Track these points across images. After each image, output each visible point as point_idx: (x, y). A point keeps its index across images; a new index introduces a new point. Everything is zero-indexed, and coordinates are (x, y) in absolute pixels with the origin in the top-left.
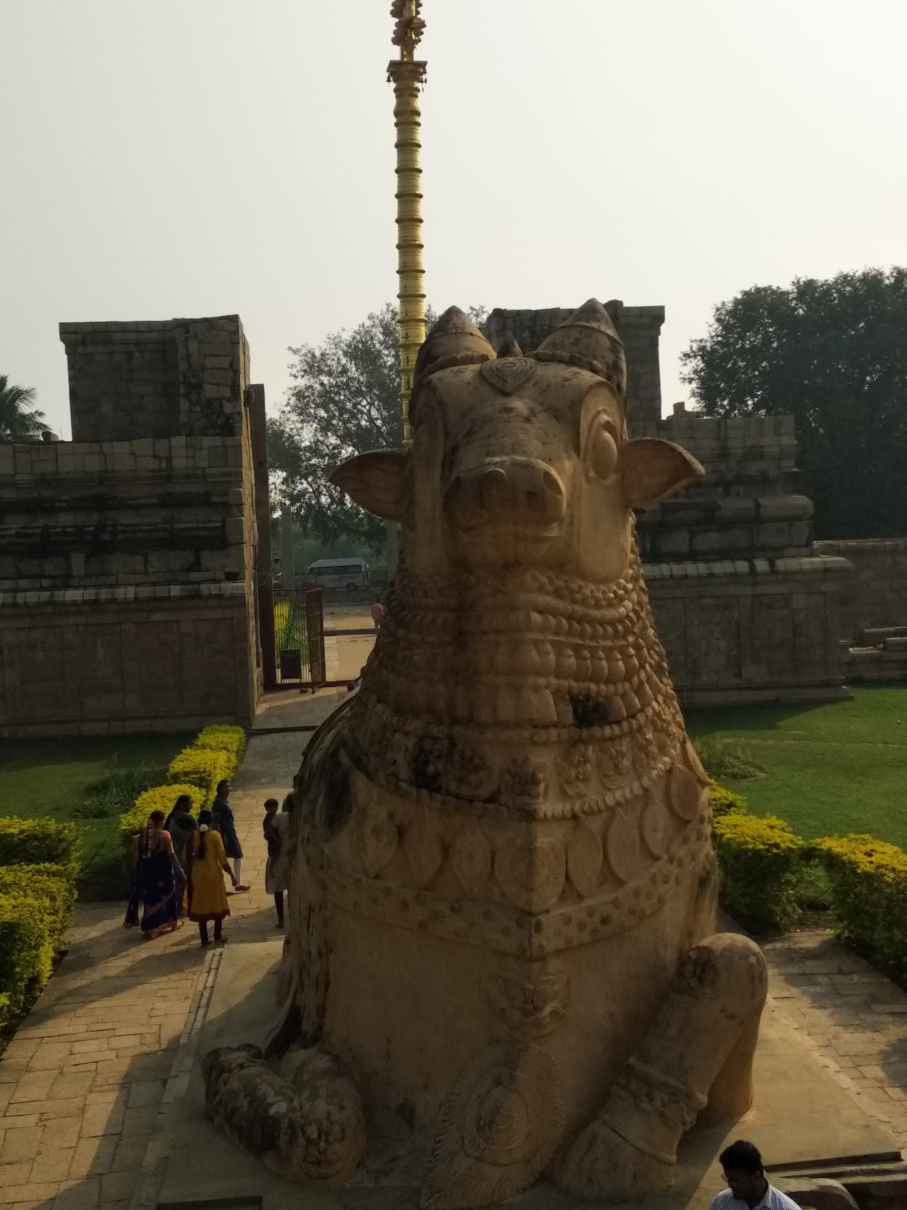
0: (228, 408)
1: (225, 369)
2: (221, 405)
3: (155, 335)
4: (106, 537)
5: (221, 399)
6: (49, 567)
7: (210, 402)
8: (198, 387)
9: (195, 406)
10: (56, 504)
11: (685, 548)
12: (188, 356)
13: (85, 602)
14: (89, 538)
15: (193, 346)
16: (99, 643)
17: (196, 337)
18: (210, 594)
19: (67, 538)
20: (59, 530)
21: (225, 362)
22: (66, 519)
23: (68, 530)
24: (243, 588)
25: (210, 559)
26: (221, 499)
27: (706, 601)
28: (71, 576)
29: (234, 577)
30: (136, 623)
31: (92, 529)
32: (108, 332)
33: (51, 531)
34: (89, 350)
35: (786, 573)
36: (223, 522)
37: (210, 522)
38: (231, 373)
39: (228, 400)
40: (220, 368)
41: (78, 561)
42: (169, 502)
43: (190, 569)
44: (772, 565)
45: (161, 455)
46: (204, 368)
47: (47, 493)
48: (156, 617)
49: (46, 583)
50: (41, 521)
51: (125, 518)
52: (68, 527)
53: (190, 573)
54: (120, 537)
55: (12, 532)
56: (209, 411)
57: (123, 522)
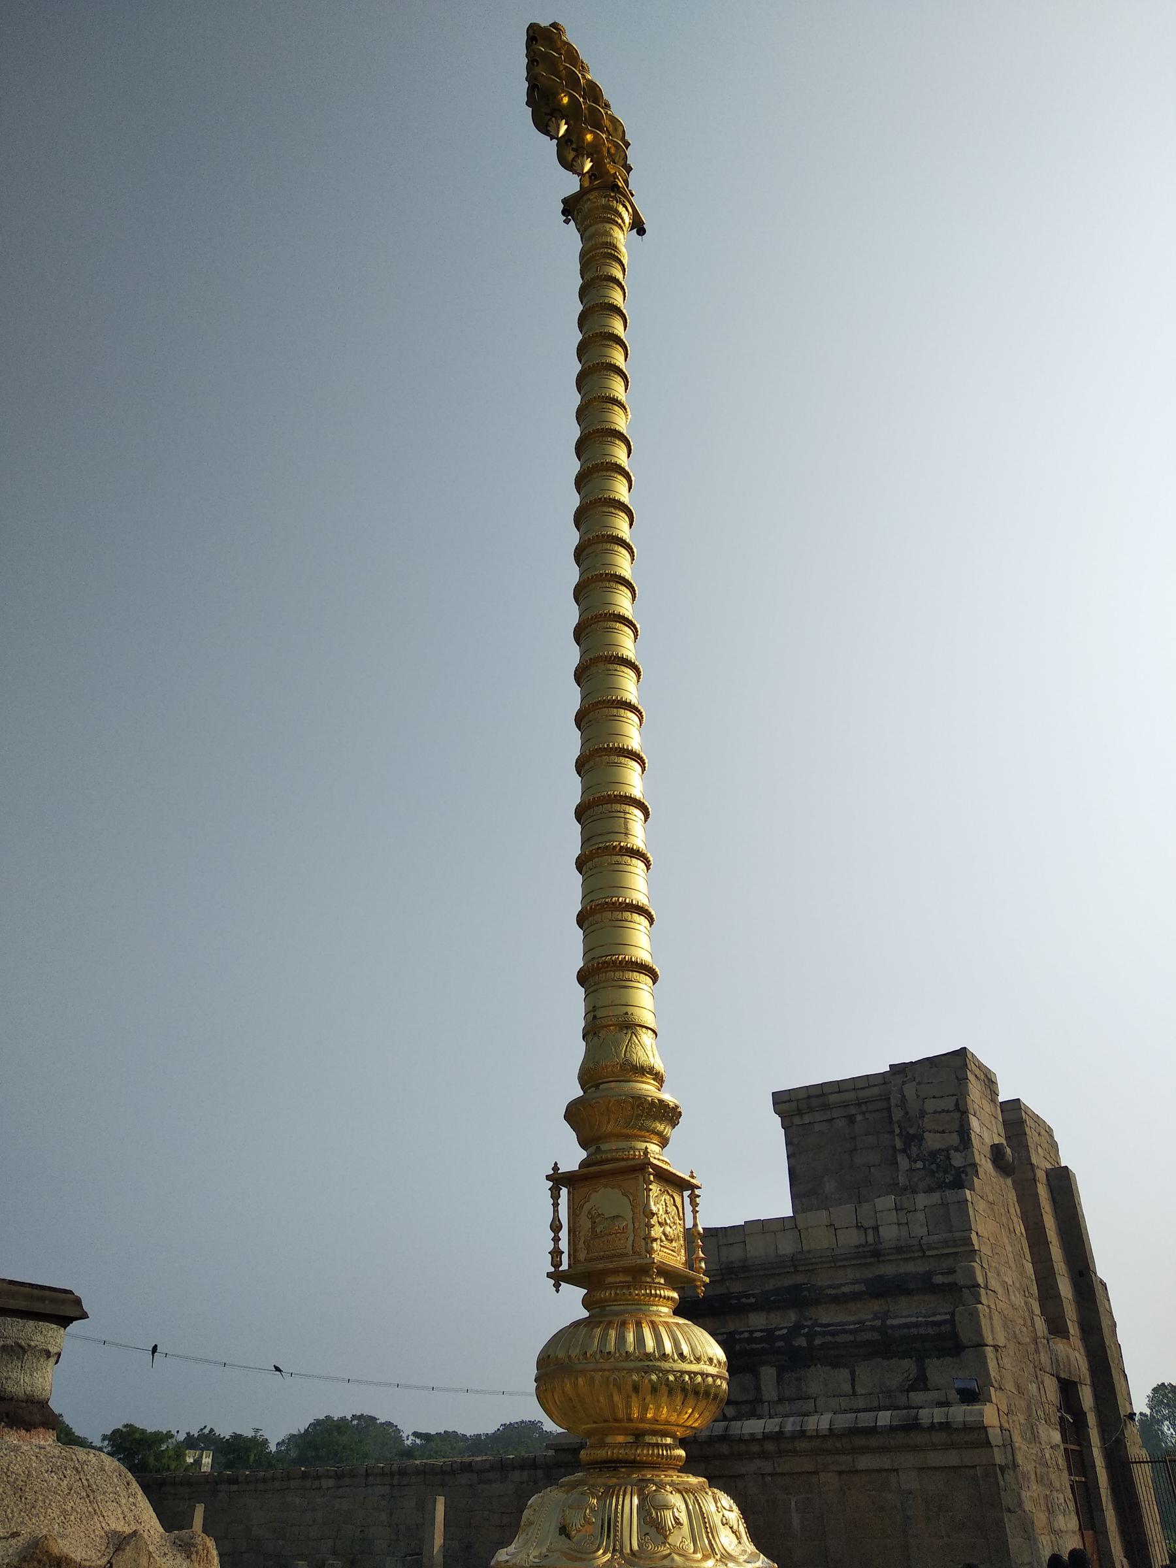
0: (957, 1160)
1: (948, 1111)
4: (801, 1342)
5: (947, 1150)
7: (933, 1154)
8: (919, 1138)
9: (915, 1162)
10: (744, 1300)
14: (781, 1344)
18: (932, 1423)
19: (754, 1346)
20: (746, 1335)
21: (949, 1104)
23: (758, 1334)
24: (981, 1414)
25: (939, 1371)
29: (971, 1396)
31: (785, 1331)
37: (934, 1315)
38: (957, 1115)
39: (956, 1150)
40: (943, 1111)
42: (882, 1289)
46: (923, 1113)
51: (827, 1316)
52: (759, 1331)
54: (818, 1341)
56: (934, 1167)
57: (824, 1320)
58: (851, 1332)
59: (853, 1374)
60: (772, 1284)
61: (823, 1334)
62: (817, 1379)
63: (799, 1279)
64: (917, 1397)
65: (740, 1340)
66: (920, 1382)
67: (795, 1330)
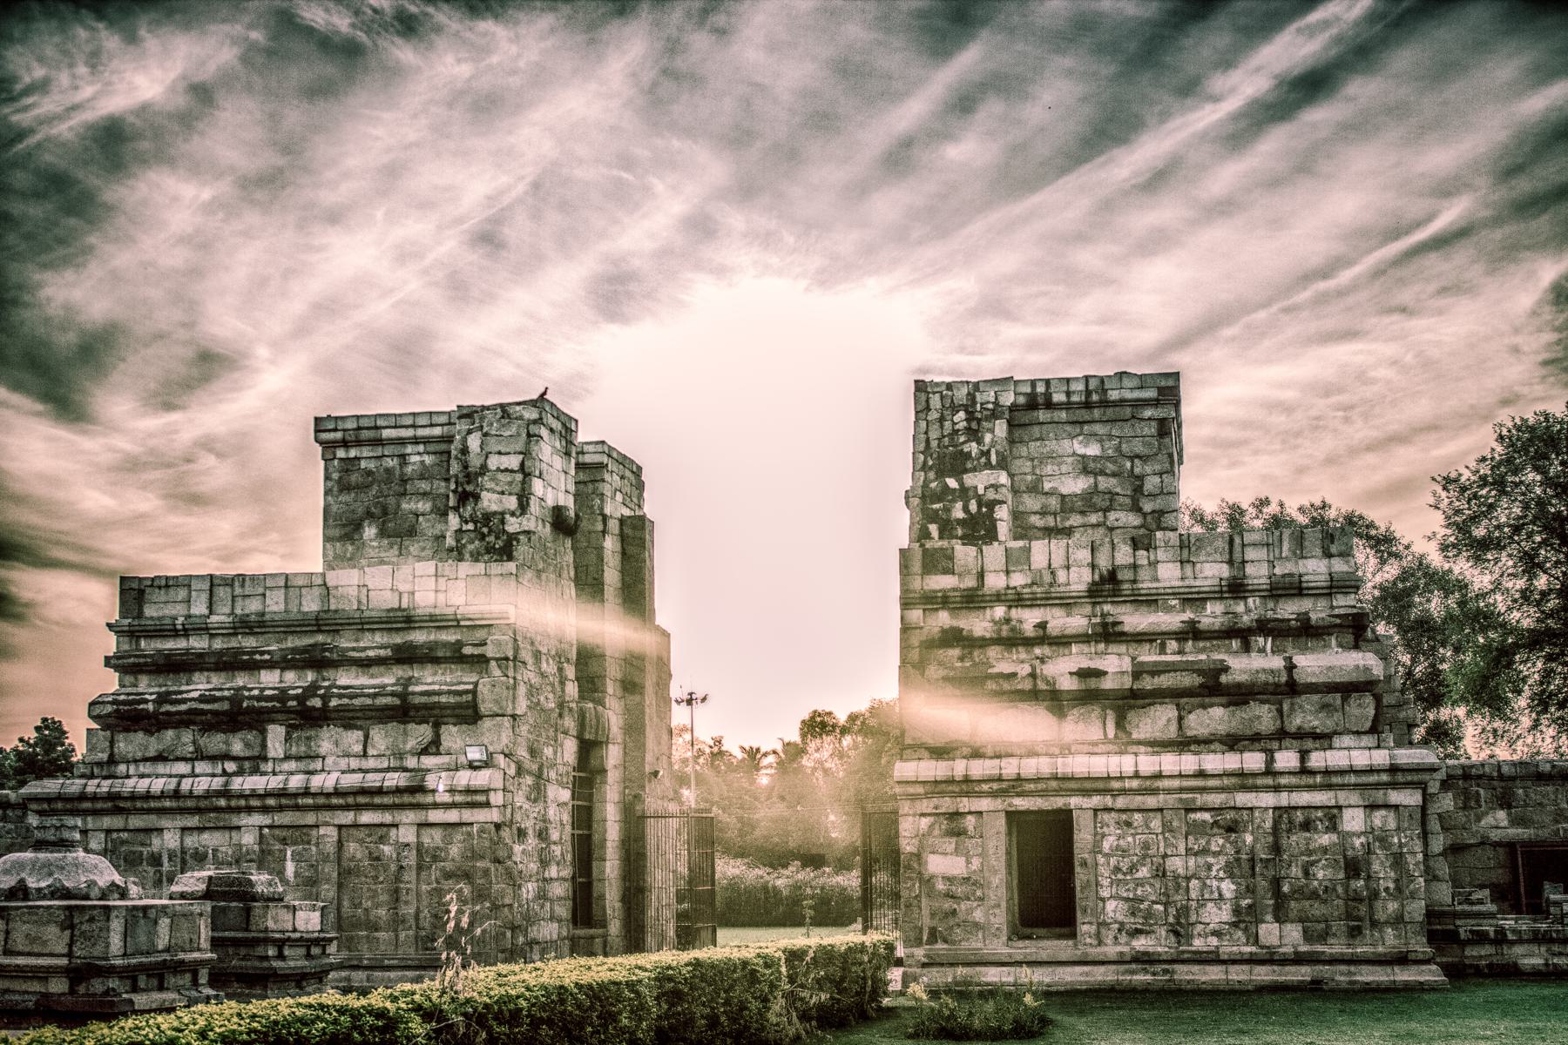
1: (512, 471)
2: (503, 522)
4: (316, 702)
5: (503, 513)
7: (488, 517)
9: (466, 522)
10: (258, 657)
11: (1172, 732)
12: (465, 451)
13: (269, 794)
14: (295, 703)
15: (474, 442)
16: (289, 853)
17: (481, 427)
20: (256, 692)
22: (270, 679)
23: (267, 693)
26: (476, 651)
27: (1199, 816)
28: (265, 759)
30: (340, 827)
31: (300, 691)
32: (377, 428)
33: (246, 693)
34: (353, 453)
35: (1327, 772)
36: (476, 684)
39: (513, 514)
40: (506, 470)
41: (276, 736)
43: (425, 751)
44: (1303, 760)
45: (401, 588)
46: (484, 469)
47: (250, 642)
48: (367, 817)
49: (231, 767)
50: (241, 680)
53: (423, 758)
54: (334, 703)
55: (195, 695)
56: (485, 530)
58: (368, 695)
59: (367, 737)
60: (293, 642)
61: (340, 696)
62: (327, 740)
65: (251, 698)
66: (433, 747)
67: (311, 690)
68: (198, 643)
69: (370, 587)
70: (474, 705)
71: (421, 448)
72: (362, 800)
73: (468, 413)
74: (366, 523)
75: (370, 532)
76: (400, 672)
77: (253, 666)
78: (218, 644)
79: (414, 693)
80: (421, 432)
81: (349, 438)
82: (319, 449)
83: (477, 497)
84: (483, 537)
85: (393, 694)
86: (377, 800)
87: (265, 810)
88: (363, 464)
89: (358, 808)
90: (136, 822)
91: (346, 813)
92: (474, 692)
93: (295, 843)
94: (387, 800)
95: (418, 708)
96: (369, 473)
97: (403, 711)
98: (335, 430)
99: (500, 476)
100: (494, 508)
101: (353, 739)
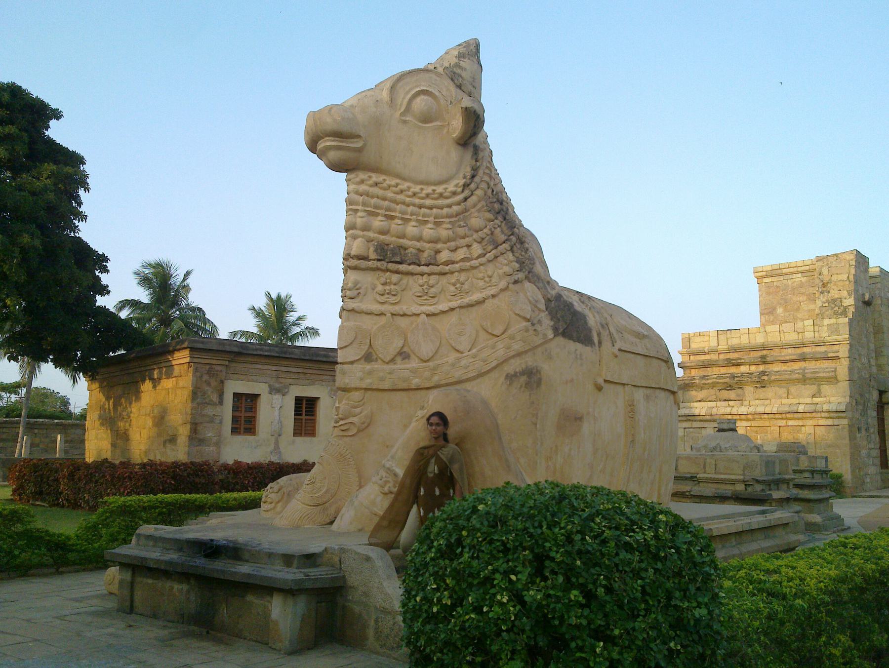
2: (841, 302)
3: (807, 268)
5: (841, 298)
6: (732, 394)
7: (834, 301)
9: (825, 303)
15: (825, 271)
16: (759, 437)
39: (845, 299)
43: (814, 396)
45: (799, 331)
48: (791, 423)
50: (733, 370)
55: (715, 376)
59: (788, 390)
62: (770, 392)
63: (764, 352)
64: (816, 400)
68: (714, 357)
69: (785, 331)
70: (836, 378)
71: (800, 275)
72: (788, 415)
73: (820, 259)
74: (778, 307)
75: (780, 310)
76: (802, 364)
77: (739, 365)
78: (722, 357)
79: (807, 373)
80: (800, 269)
81: (768, 274)
82: (756, 279)
83: (829, 292)
84: (832, 308)
85: (798, 373)
86: (796, 415)
87: (748, 420)
88: (775, 284)
89: (787, 419)
90: (695, 425)
91: (782, 421)
92: (835, 371)
93: (761, 433)
94: (800, 415)
95: (810, 379)
96: (778, 287)
97: (804, 380)
98: (763, 271)
99: (838, 283)
100: (836, 296)
101: (782, 392)
